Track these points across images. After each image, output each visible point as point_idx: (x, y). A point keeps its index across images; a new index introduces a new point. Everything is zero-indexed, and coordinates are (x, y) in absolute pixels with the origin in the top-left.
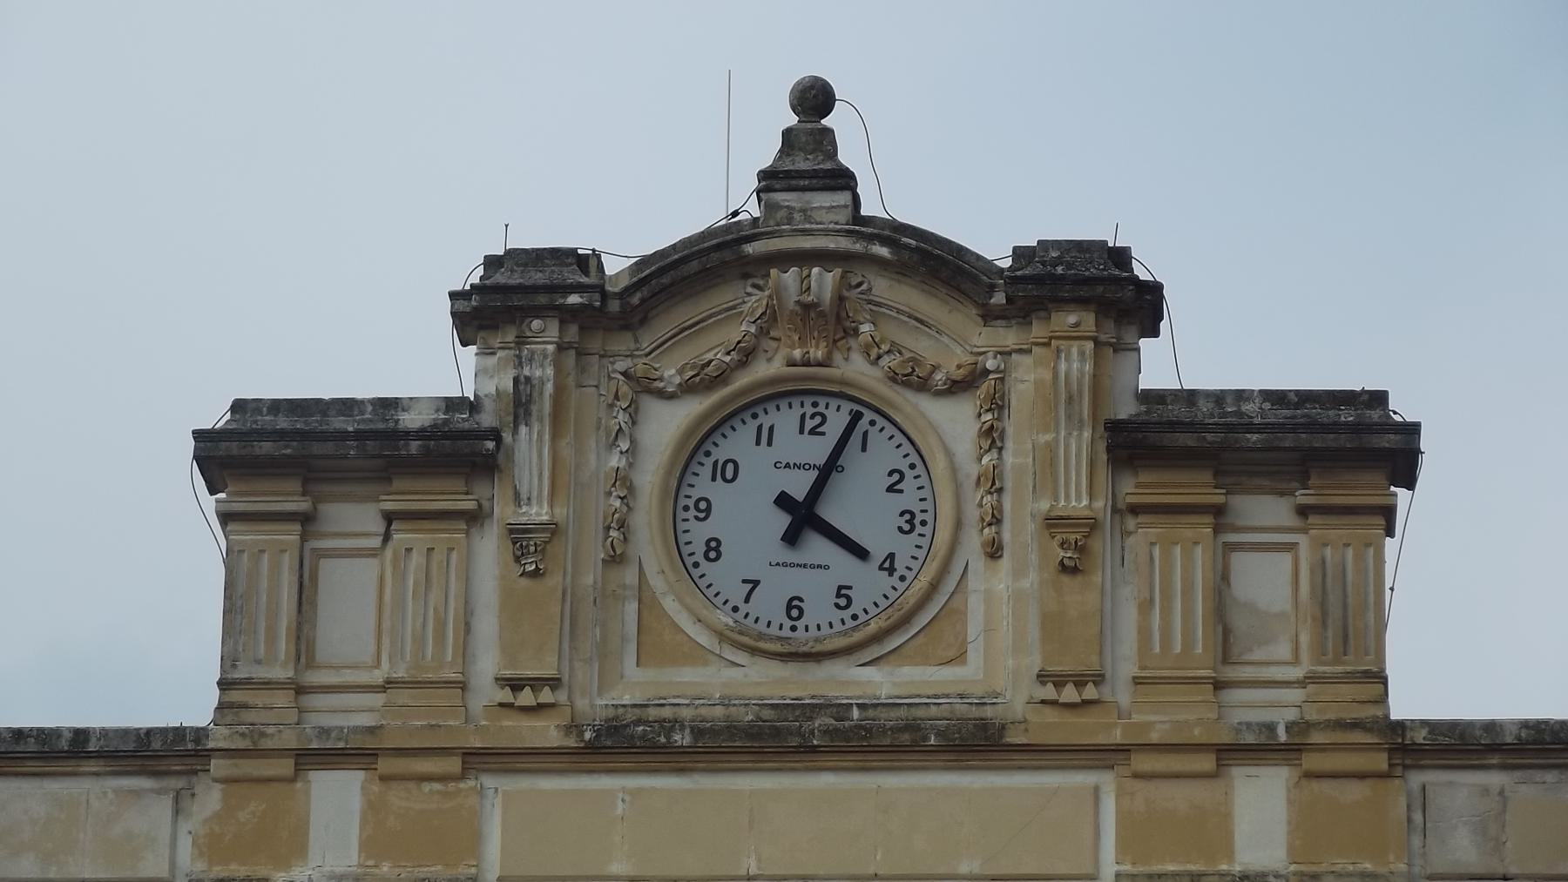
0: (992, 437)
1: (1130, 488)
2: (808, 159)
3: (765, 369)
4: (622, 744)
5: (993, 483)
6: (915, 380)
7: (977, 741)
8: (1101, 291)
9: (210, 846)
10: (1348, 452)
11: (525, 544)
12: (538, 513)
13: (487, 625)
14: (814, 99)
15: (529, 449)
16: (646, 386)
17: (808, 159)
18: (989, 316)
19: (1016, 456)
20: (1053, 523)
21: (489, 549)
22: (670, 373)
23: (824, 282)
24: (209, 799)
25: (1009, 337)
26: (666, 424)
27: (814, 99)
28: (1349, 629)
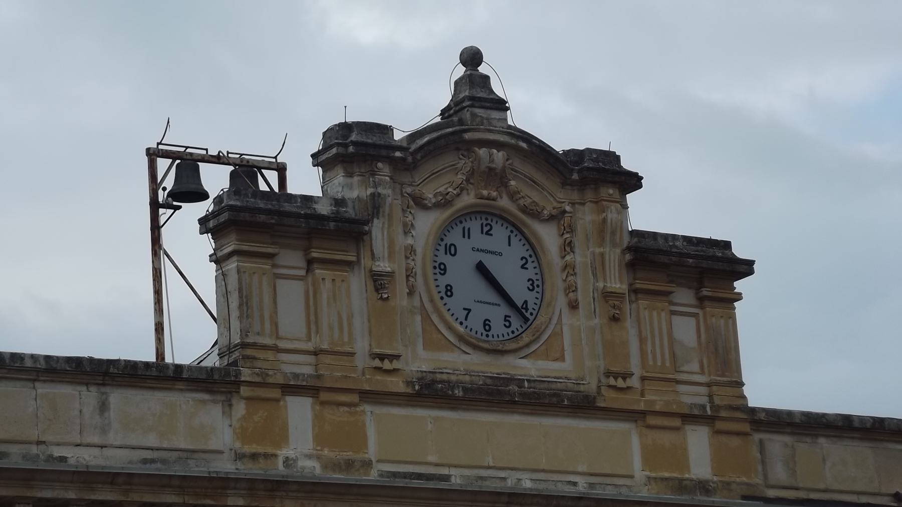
0: (568, 247)
3: (468, 199)
4: (431, 392)
5: (569, 269)
7: (582, 405)
8: (603, 176)
9: (243, 435)
10: (708, 270)
12: (384, 266)
15: (377, 230)
16: (419, 202)
18: (566, 183)
19: (580, 258)
20: (607, 295)
22: (429, 194)
23: (499, 156)
24: (240, 408)
25: (575, 196)
26: (426, 224)
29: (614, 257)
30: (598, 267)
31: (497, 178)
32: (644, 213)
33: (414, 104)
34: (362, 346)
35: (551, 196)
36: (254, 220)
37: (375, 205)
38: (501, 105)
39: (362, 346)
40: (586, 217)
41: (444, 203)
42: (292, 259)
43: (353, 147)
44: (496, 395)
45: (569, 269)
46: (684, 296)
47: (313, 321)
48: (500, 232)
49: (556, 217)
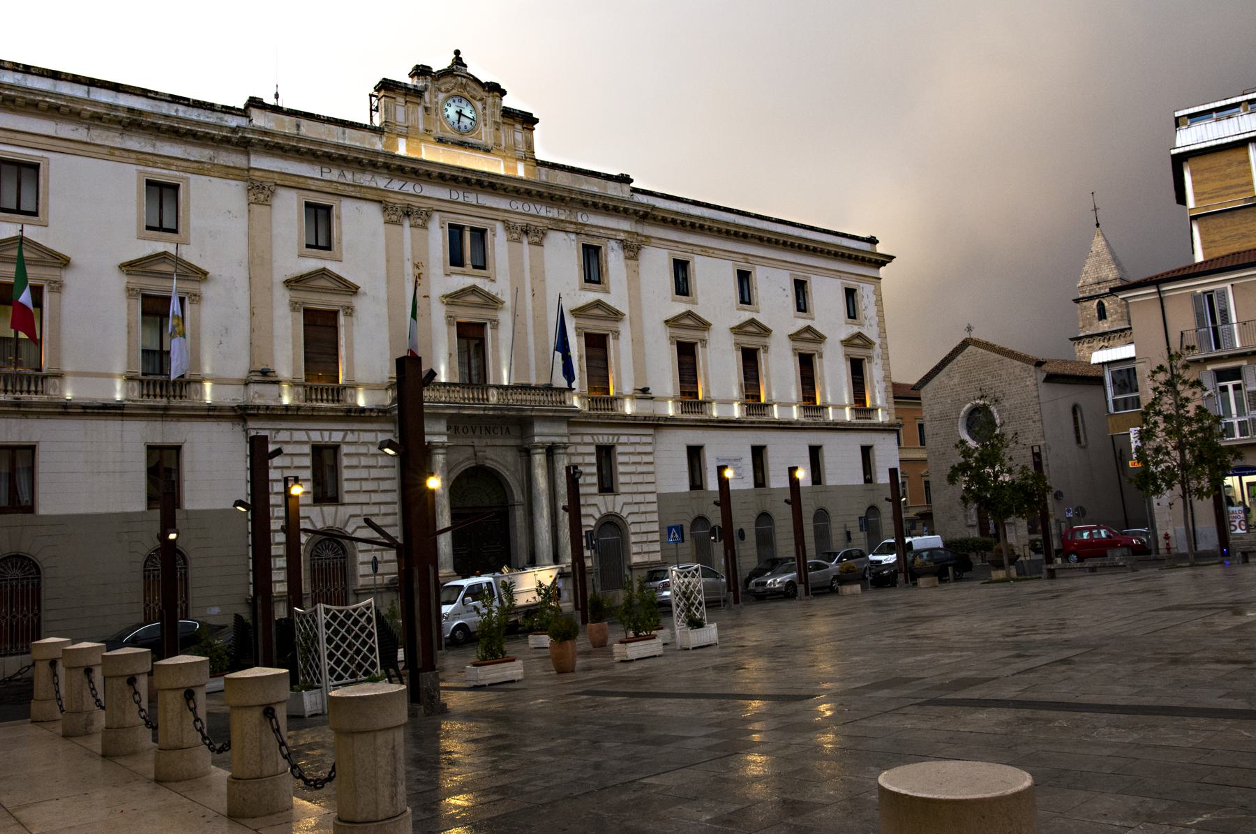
1: (506, 120)
2: (458, 60)
3: (454, 92)
5: (485, 115)
6: (474, 98)
8: (496, 89)
10: (528, 121)
11: (426, 109)
13: (421, 121)
14: (457, 52)
15: (426, 95)
16: (440, 90)
17: (458, 60)
20: (495, 122)
21: (420, 109)
23: (464, 80)
24: (384, 139)
27: (457, 52)
28: (530, 146)
29: (498, 113)
30: (493, 114)
31: (464, 87)
32: (507, 102)
33: (440, 62)
34: (421, 127)
35: (480, 93)
36: (387, 86)
37: (426, 88)
38: (465, 66)
39: (421, 127)
40: (490, 101)
41: (447, 91)
42: (401, 100)
43: (421, 71)
44: (462, 145)
45: (485, 115)
46: (519, 127)
47: (407, 119)
48: (464, 102)
49: (481, 100)
